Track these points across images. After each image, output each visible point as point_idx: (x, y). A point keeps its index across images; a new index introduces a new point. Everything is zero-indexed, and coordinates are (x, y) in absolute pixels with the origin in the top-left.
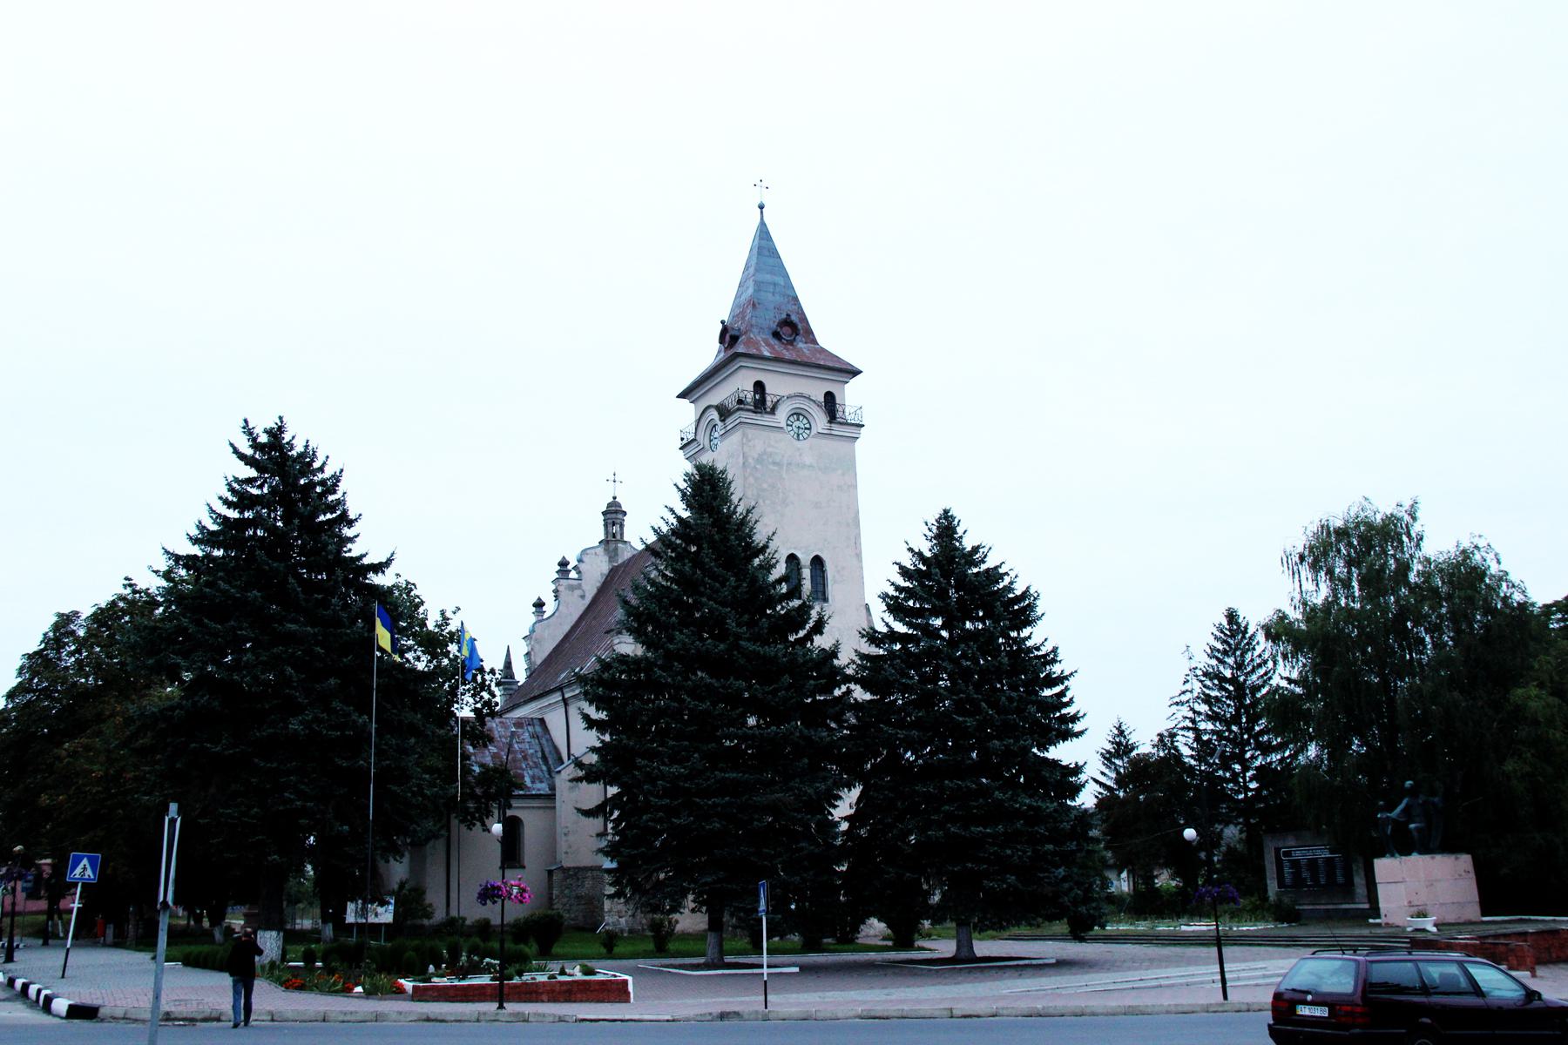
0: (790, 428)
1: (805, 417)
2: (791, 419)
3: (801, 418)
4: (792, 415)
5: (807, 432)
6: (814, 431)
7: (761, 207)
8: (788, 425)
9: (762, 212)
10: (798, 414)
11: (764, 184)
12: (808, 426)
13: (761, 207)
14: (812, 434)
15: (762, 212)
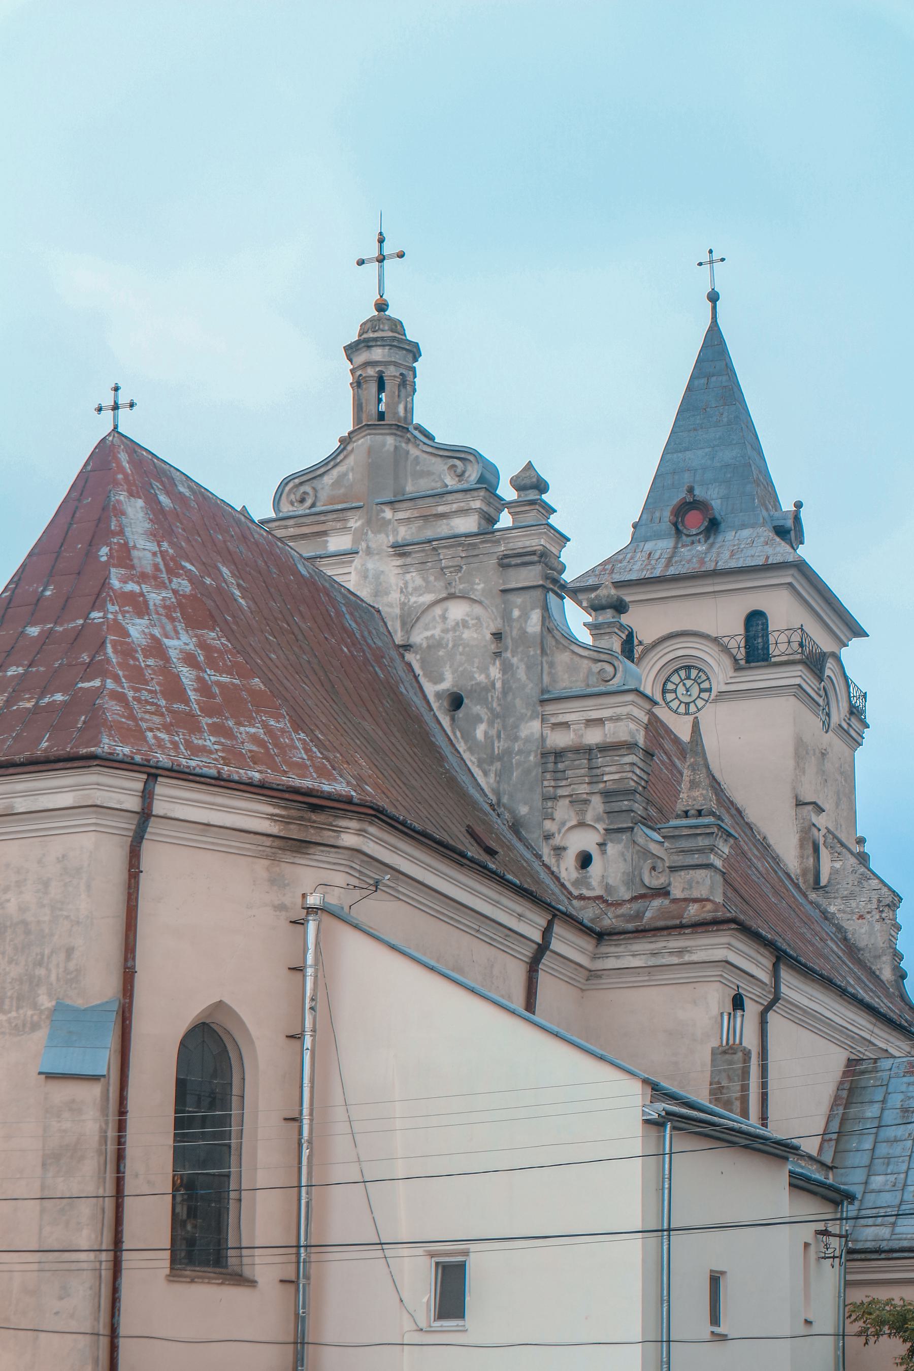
0: (670, 696)
1: (700, 670)
2: (675, 679)
3: (694, 673)
4: (676, 671)
5: (705, 695)
6: (714, 693)
7: (713, 297)
8: (664, 691)
9: (714, 308)
10: (688, 668)
11: (716, 256)
12: (706, 685)
13: (713, 297)
14: (712, 697)
15: (714, 308)
